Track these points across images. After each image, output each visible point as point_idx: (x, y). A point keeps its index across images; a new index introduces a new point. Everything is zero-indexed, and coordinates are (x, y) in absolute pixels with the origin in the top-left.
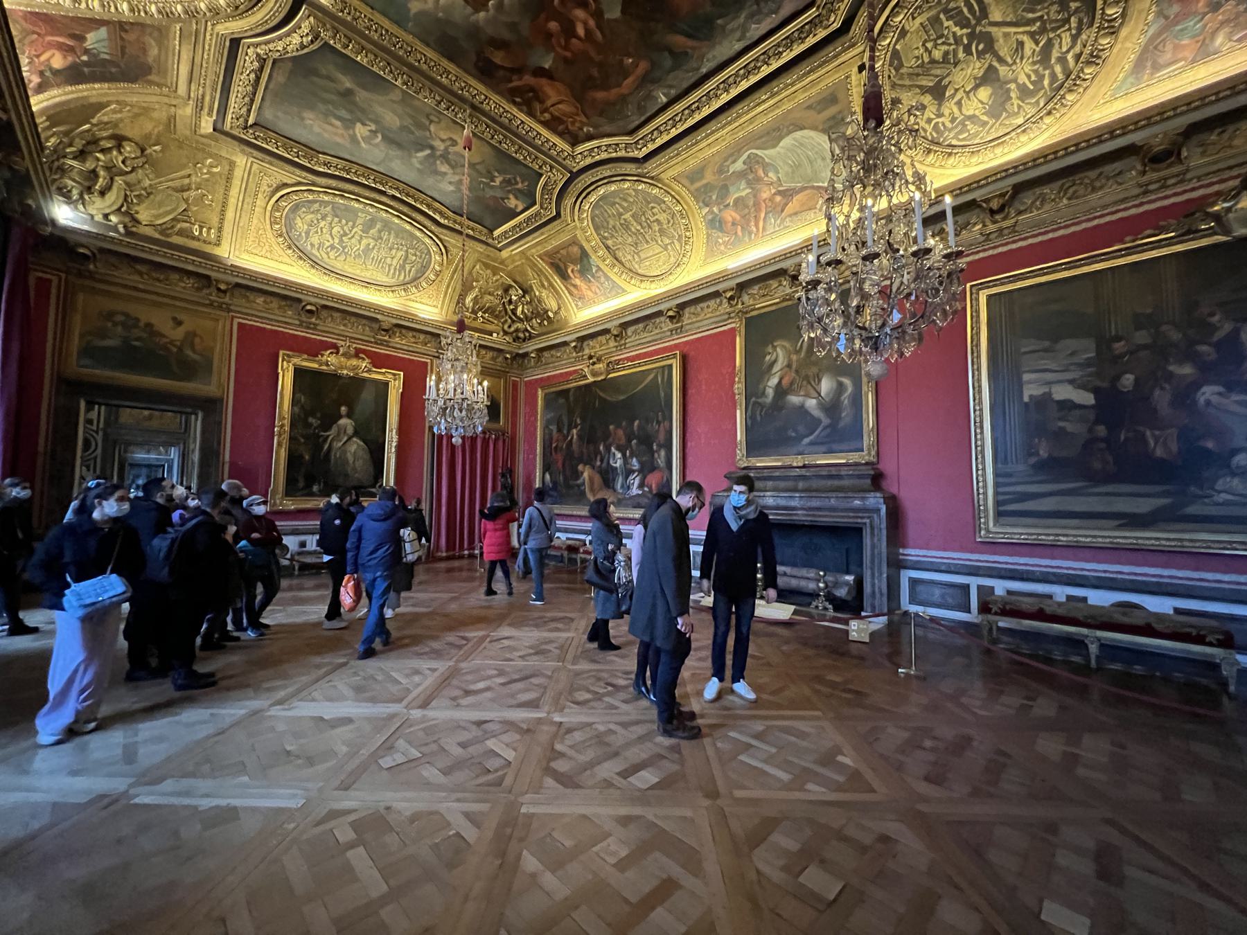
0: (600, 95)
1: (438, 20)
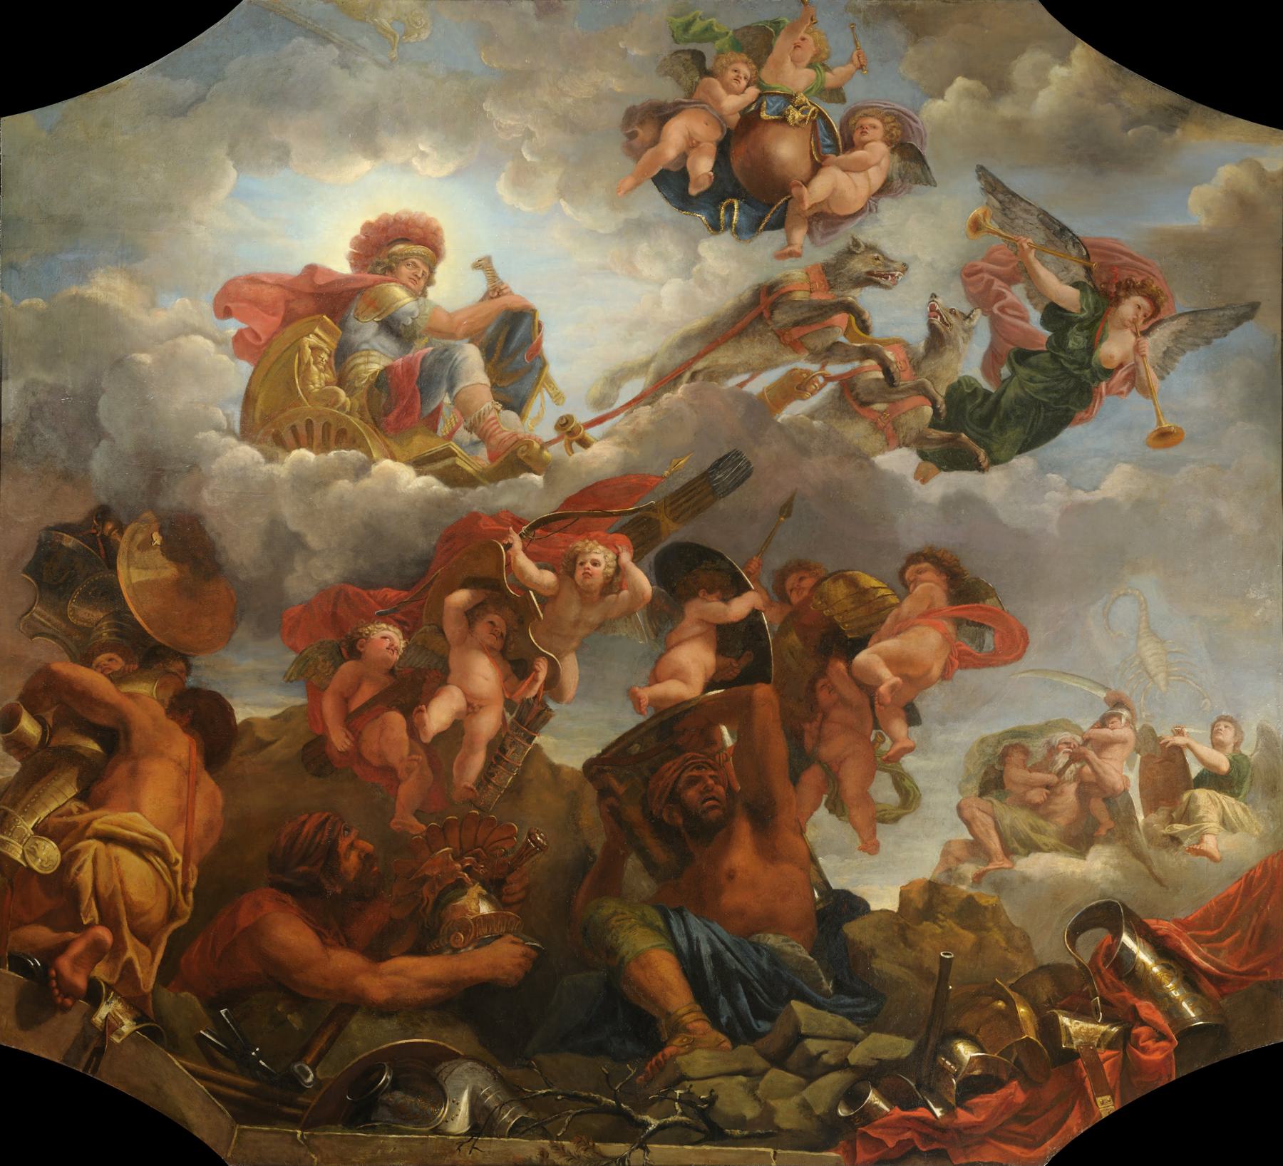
0: (292, 935)
1: (119, 363)
